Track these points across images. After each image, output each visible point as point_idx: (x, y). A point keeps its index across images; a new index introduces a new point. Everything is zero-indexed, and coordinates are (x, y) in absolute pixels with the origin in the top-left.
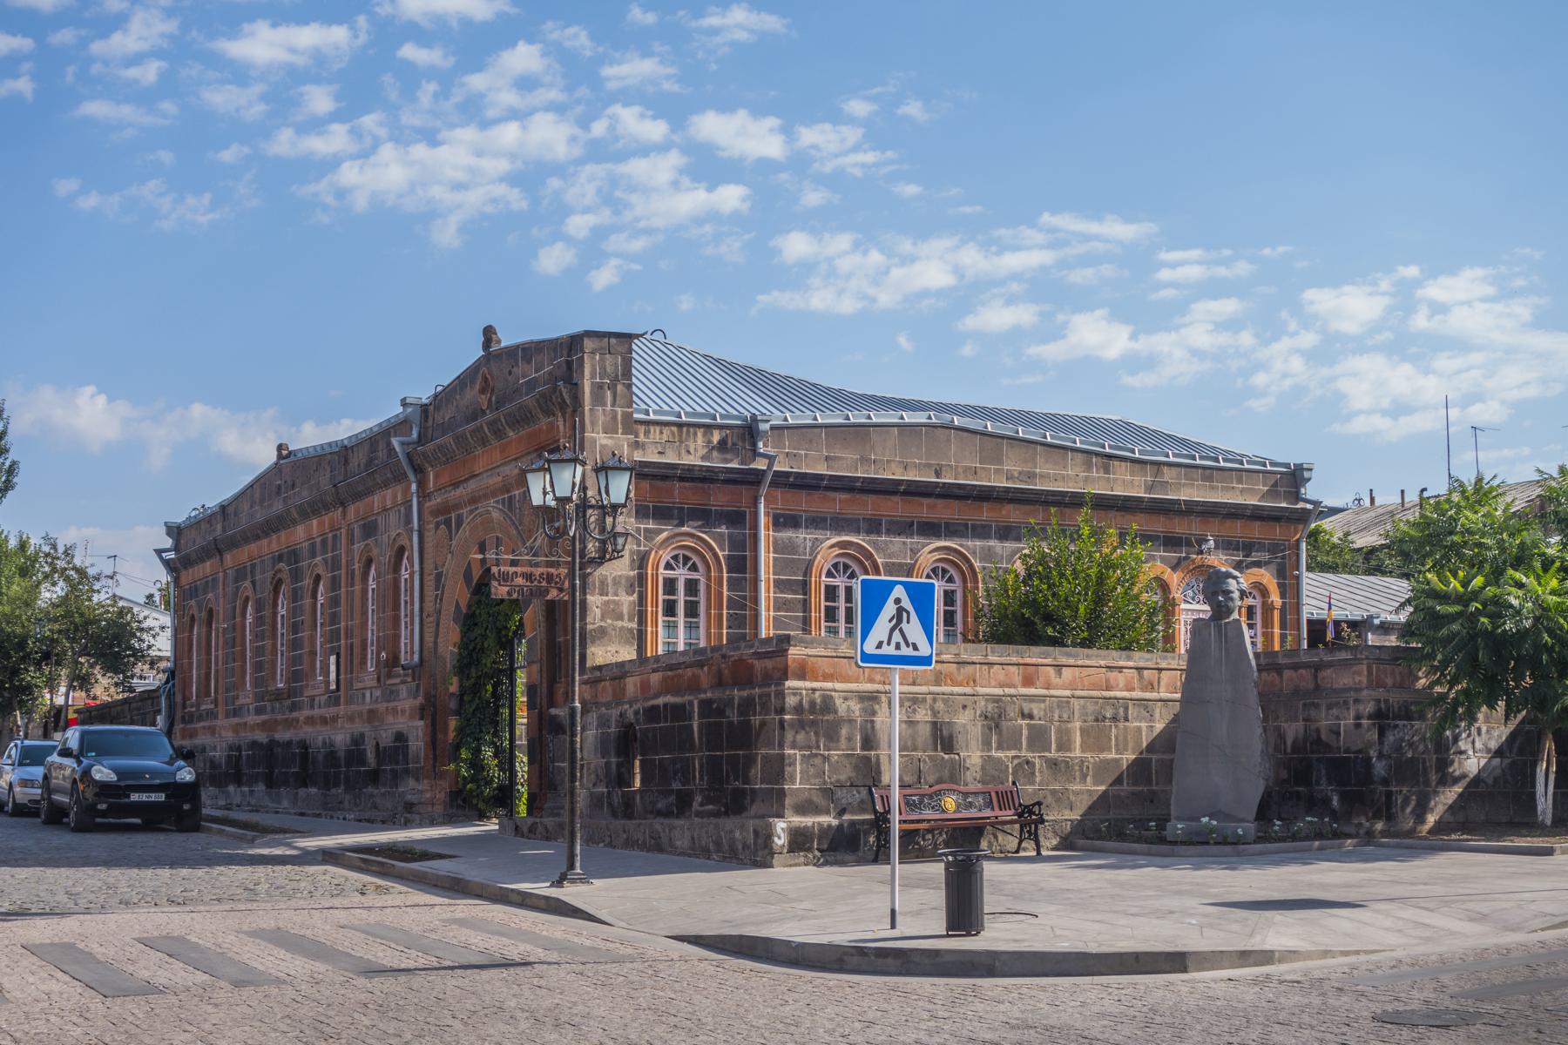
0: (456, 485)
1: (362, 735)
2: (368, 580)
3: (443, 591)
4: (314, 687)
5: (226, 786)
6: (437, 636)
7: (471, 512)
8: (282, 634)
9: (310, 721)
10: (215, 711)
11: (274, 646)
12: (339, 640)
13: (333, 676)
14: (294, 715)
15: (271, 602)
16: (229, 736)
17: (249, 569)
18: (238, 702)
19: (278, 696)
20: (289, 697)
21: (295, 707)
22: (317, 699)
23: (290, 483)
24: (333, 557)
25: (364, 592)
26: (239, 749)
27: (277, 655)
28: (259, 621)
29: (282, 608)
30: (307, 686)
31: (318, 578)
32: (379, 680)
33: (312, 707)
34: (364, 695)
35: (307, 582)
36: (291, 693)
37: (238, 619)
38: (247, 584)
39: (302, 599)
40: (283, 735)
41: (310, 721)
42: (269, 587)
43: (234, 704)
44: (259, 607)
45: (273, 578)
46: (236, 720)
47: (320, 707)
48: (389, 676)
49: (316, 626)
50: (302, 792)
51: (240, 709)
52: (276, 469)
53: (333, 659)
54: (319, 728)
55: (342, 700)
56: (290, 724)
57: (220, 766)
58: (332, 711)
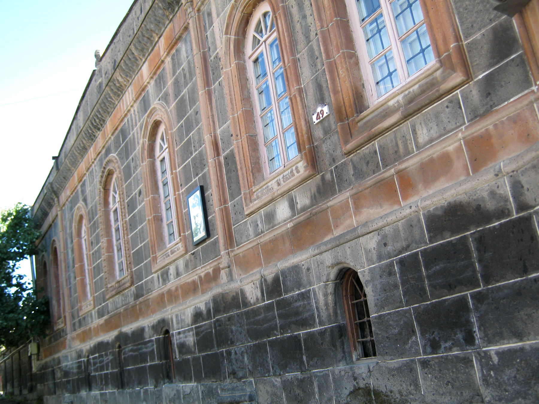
5: (79, 391)
8: (117, 230)
10: (65, 328)
11: (110, 242)
18: (81, 313)
20: (132, 284)
22: (172, 270)
27: (113, 251)
29: (114, 202)
30: (155, 259)
34: (270, 217)
39: (136, 168)
43: (78, 316)
45: (102, 177)
47: (178, 274)
51: (84, 318)
53: (195, 200)
58: (207, 268)
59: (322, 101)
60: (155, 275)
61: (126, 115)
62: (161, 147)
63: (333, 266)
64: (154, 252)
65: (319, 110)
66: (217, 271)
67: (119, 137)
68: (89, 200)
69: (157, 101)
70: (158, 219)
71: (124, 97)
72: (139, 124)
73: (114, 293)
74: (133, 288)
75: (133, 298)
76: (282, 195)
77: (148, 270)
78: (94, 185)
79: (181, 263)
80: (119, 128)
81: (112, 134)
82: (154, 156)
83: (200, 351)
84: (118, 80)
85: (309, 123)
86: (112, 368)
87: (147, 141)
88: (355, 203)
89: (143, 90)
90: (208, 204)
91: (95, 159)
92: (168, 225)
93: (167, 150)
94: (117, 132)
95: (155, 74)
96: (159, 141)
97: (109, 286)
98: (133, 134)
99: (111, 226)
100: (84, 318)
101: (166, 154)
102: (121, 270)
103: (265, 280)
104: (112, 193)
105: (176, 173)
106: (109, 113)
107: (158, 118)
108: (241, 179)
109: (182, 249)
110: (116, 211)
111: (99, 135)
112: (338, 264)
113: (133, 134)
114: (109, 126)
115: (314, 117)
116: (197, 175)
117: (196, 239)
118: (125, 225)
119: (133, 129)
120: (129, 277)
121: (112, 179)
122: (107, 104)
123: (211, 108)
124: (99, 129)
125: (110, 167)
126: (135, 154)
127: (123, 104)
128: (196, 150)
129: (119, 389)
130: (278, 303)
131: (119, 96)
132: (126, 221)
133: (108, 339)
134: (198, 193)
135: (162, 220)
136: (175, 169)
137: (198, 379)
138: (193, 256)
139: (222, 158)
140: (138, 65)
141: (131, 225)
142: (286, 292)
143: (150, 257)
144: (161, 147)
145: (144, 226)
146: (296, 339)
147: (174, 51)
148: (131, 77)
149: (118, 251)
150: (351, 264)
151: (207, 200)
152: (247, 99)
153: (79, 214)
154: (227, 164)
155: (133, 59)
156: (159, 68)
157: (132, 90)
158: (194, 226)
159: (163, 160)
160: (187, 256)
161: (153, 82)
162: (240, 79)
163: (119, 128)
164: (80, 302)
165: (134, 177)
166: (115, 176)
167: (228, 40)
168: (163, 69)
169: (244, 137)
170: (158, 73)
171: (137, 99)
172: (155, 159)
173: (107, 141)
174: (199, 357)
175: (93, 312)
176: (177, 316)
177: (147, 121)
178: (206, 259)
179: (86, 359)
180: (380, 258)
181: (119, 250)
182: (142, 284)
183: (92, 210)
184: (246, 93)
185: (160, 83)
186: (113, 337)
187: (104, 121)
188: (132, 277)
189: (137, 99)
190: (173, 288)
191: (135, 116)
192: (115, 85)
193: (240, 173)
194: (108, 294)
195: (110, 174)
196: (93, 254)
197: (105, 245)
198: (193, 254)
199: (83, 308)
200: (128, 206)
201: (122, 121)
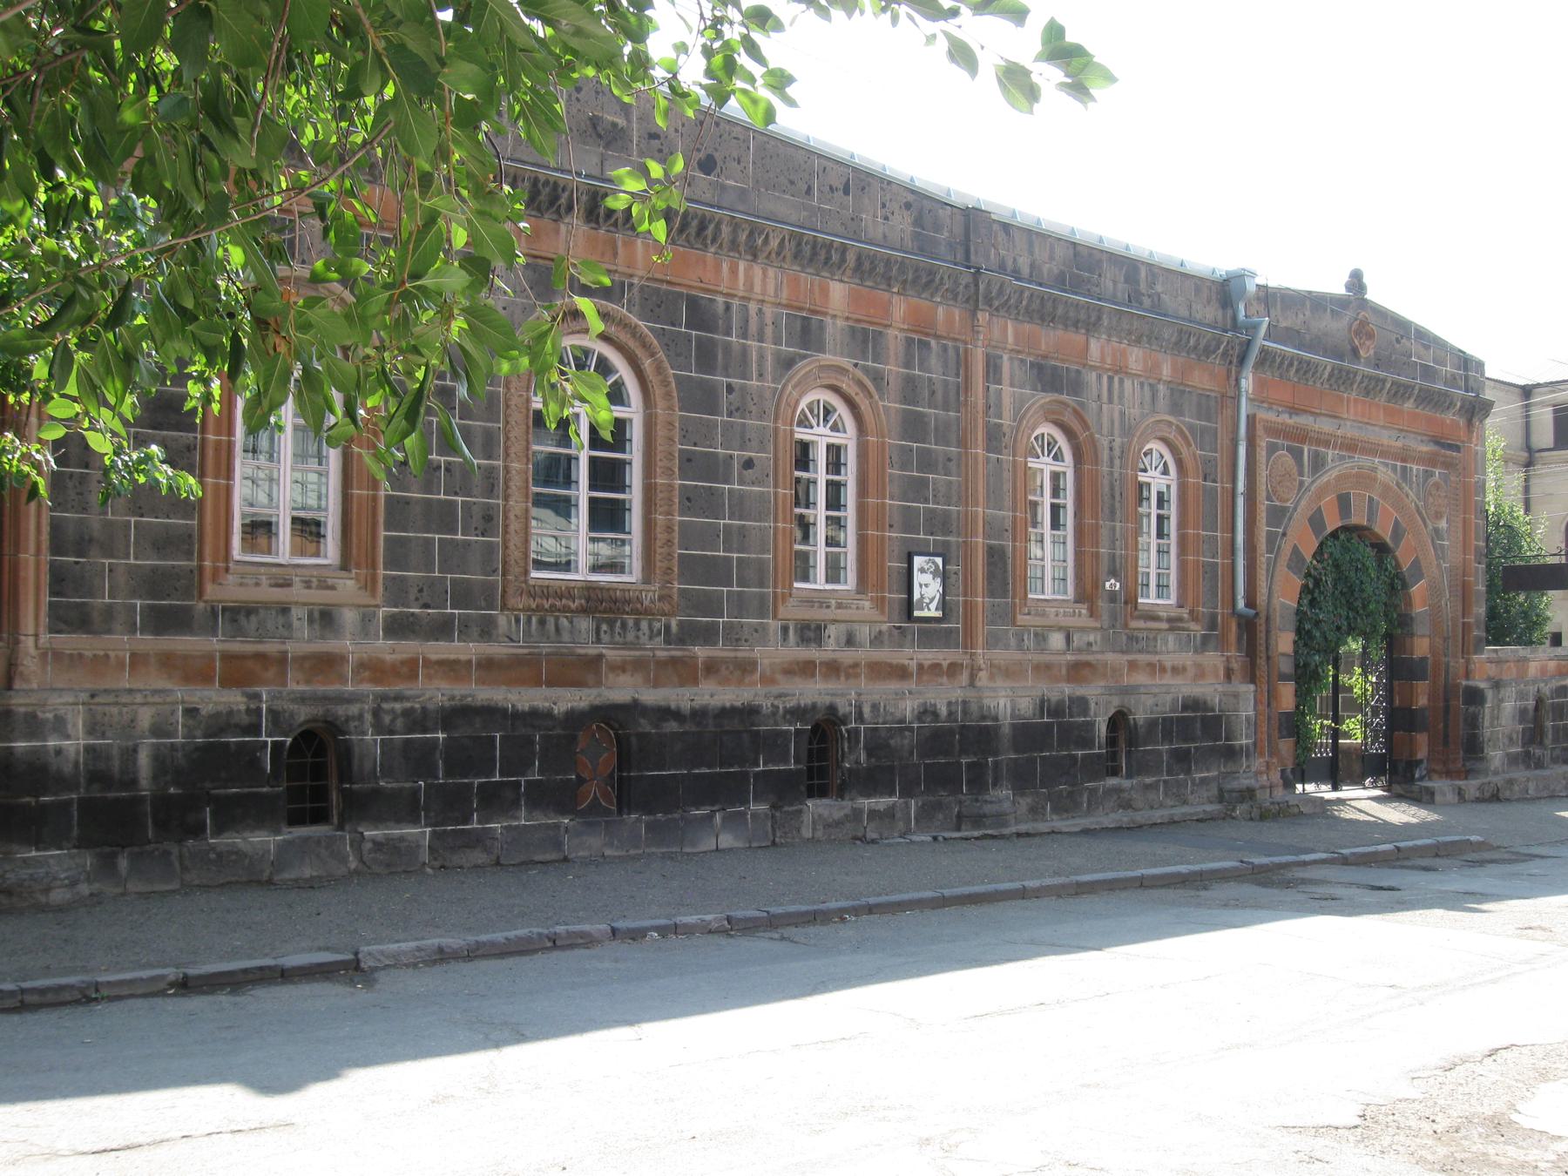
76: (1060, 629)
138: (896, 632)
142: (1071, 716)
146: (1074, 758)
174: (919, 765)
180: (1152, 713)
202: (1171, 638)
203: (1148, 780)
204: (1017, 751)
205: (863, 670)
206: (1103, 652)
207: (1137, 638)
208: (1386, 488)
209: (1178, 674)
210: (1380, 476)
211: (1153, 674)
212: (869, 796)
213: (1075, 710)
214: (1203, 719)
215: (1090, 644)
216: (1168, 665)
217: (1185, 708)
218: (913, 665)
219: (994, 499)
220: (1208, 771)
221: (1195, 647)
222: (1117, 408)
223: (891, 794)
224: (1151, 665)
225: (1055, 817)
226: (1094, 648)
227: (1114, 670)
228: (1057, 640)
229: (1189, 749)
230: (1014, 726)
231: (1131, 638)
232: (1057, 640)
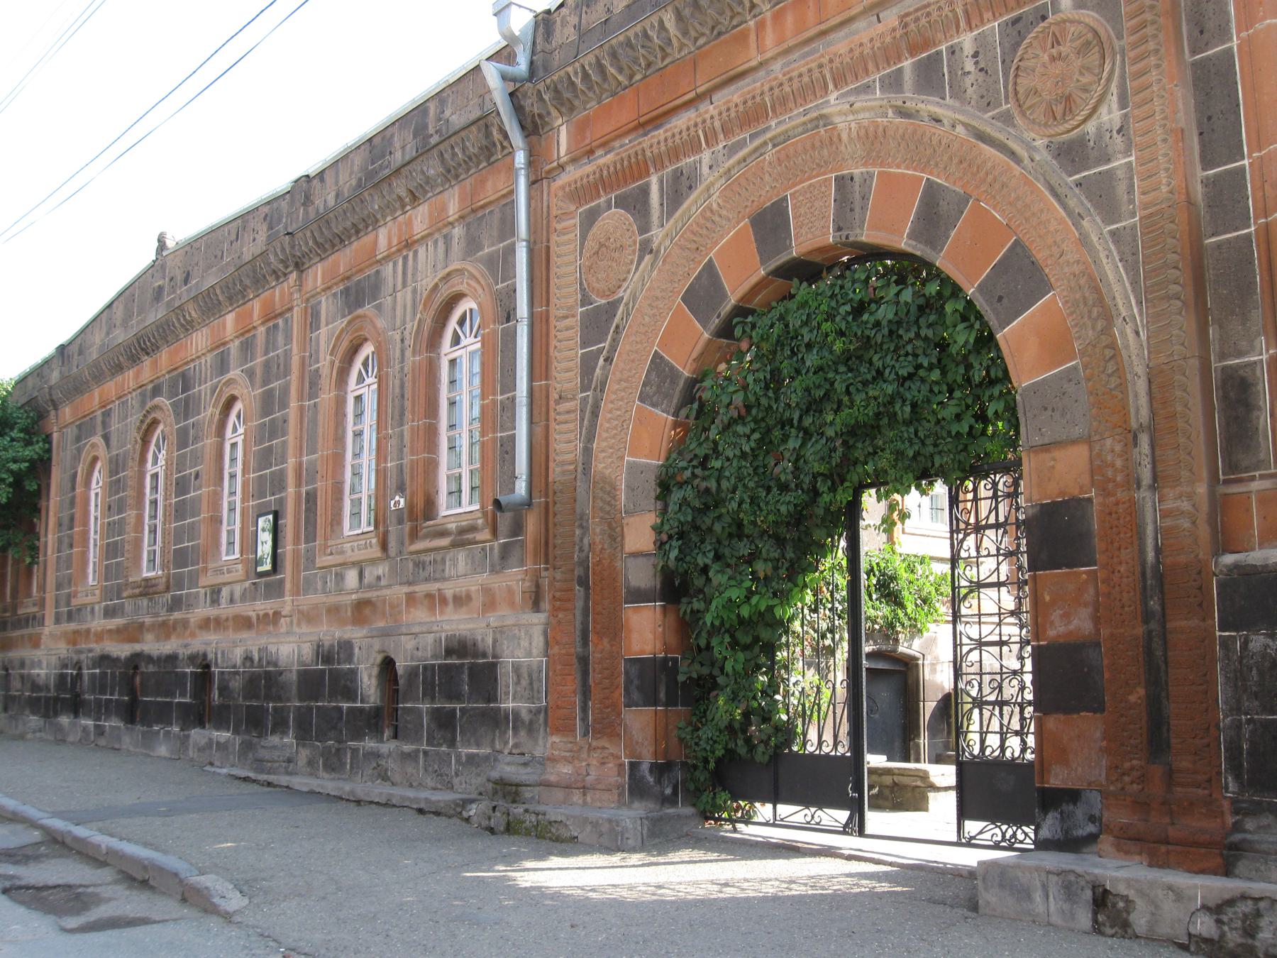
0: (655, 121)
1: (346, 646)
2: (346, 383)
3: (615, 341)
4: (219, 571)
5: (56, 714)
6: (590, 438)
7: (732, 150)
9: (206, 624)
10: (38, 615)
11: (140, 518)
12: (283, 488)
13: (265, 548)
14: (177, 615)
15: (137, 456)
16: (63, 649)
17: (99, 419)
18: (74, 602)
19: (148, 589)
20: (168, 589)
21: (176, 604)
22: (225, 592)
23: (180, 277)
24: (267, 365)
25: (340, 403)
26: (78, 665)
28: (115, 486)
30: (205, 570)
31: (232, 401)
32: (384, 546)
33: (215, 601)
34: (340, 577)
35: (209, 412)
36: (173, 583)
37: (79, 490)
38: (97, 439)
39: (196, 439)
40: (152, 646)
41: (206, 624)
42: (134, 435)
43: (68, 604)
44: (115, 466)
45: (142, 422)
46: (73, 626)
47: (232, 601)
48: (414, 535)
49: (222, 479)
50: (198, 735)
51: (79, 610)
52: (157, 267)
53: (265, 522)
54: (231, 635)
55: (288, 586)
56: (166, 629)
57: (47, 688)
59: (401, 489)
60: (202, 591)
61: (193, 360)
62: (235, 430)
63: (379, 652)
64: (205, 561)
65: (397, 498)
66: (277, 614)
67: (178, 381)
68: (114, 441)
69: (238, 371)
70: (216, 520)
71: (194, 335)
72: (209, 384)
73: (137, 591)
74: (168, 596)
75: (165, 609)
76: (354, 564)
77: (194, 580)
78: (126, 425)
79: (238, 590)
80: (180, 370)
81: (169, 372)
82: (224, 434)
83: (245, 698)
84: (190, 313)
85: (387, 506)
86: (121, 694)
87: (218, 413)
88: (407, 602)
89: (224, 344)
90: (280, 535)
91: (134, 390)
92: (228, 531)
93: (242, 437)
94: (175, 373)
95: (242, 334)
96: (233, 417)
97: (131, 580)
98: (200, 391)
99: (144, 494)
100: (79, 610)
101: (240, 440)
102: (152, 561)
103: (323, 645)
104: (152, 447)
105: (248, 479)
106: (167, 342)
107: (236, 393)
108: (318, 527)
109: (241, 572)
110: (155, 476)
111: (147, 362)
112: (384, 651)
113: (200, 391)
114: (164, 356)
115: (392, 502)
116: (273, 494)
117: (260, 569)
118: (168, 508)
119: (200, 385)
120: (164, 580)
121: (156, 428)
122: (168, 332)
123: (301, 429)
124: (148, 354)
125: (157, 415)
126: (198, 420)
127: (192, 344)
128: (276, 465)
129: (126, 723)
130: (330, 670)
131: (187, 330)
132: (171, 504)
133: (119, 653)
134: (271, 517)
135: (221, 522)
136: (249, 474)
137: (236, 732)
139: (304, 490)
140: (220, 311)
141: (176, 511)
142: (339, 663)
143: (198, 564)
144: (235, 430)
145: (197, 522)
146: (340, 709)
147: (271, 324)
148: (209, 318)
149: (150, 532)
150: (393, 656)
151: (280, 529)
152: (339, 439)
153: (92, 454)
154: (307, 501)
155: (215, 302)
156: (248, 331)
157: (207, 334)
158: (259, 554)
159: (234, 445)
160: (247, 584)
161: (237, 342)
162: (336, 414)
163: (180, 370)
164: (76, 585)
165: (192, 450)
166: (161, 427)
167: (332, 363)
168: (254, 335)
169: (330, 482)
170: (247, 335)
171: (213, 350)
172: (224, 440)
173: (158, 378)
174: (242, 706)
175: (97, 608)
176: (223, 653)
177: (221, 389)
178: (267, 596)
179: (75, 672)
180: (412, 659)
181: (153, 531)
182: (181, 595)
183: (117, 460)
184: (340, 432)
185: (247, 349)
186: (128, 653)
187: (158, 348)
188: (168, 581)
189: (213, 350)
190: (224, 617)
191: (206, 369)
192: (184, 316)
193: (319, 520)
194: (126, 589)
195: (155, 423)
196: (109, 524)
197: (132, 521)
198: (254, 584)
199: (79, 595)
200: (177, 484)
201: (186, 363)
202: (461, 556)
203: (408, 748)
204: (301, 700)
205: (231, 623)
206: (389, 586)
207: (424, 563)
208: (872, 139)
209: (461, 605)
210: (845, 124)
211: (432, 608)
212: (218, 729)
213: (342, 656)
214: (472, 668)
215: (379, 578)
216: (449, 594)
217: (449, 652)
218: (253, 614)
219: (309, 442)
220: (478, 745)
221: (492, 566)
222: (409, 289)
223: (228, 730)
224: (429, 596)
225: (326, 775)
226: (383, 583)
227: (392, 607)
228: (351, 577)
229: (455, 709)
230: (298, 671)
231: (419, 565)
232: (351, 577)
